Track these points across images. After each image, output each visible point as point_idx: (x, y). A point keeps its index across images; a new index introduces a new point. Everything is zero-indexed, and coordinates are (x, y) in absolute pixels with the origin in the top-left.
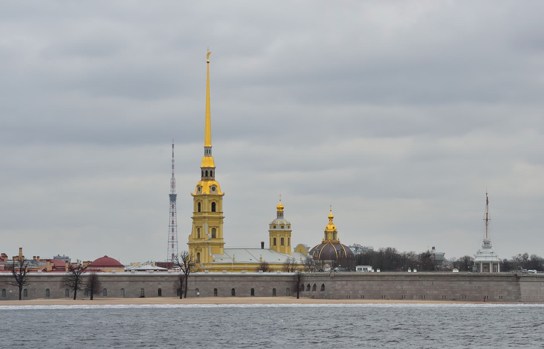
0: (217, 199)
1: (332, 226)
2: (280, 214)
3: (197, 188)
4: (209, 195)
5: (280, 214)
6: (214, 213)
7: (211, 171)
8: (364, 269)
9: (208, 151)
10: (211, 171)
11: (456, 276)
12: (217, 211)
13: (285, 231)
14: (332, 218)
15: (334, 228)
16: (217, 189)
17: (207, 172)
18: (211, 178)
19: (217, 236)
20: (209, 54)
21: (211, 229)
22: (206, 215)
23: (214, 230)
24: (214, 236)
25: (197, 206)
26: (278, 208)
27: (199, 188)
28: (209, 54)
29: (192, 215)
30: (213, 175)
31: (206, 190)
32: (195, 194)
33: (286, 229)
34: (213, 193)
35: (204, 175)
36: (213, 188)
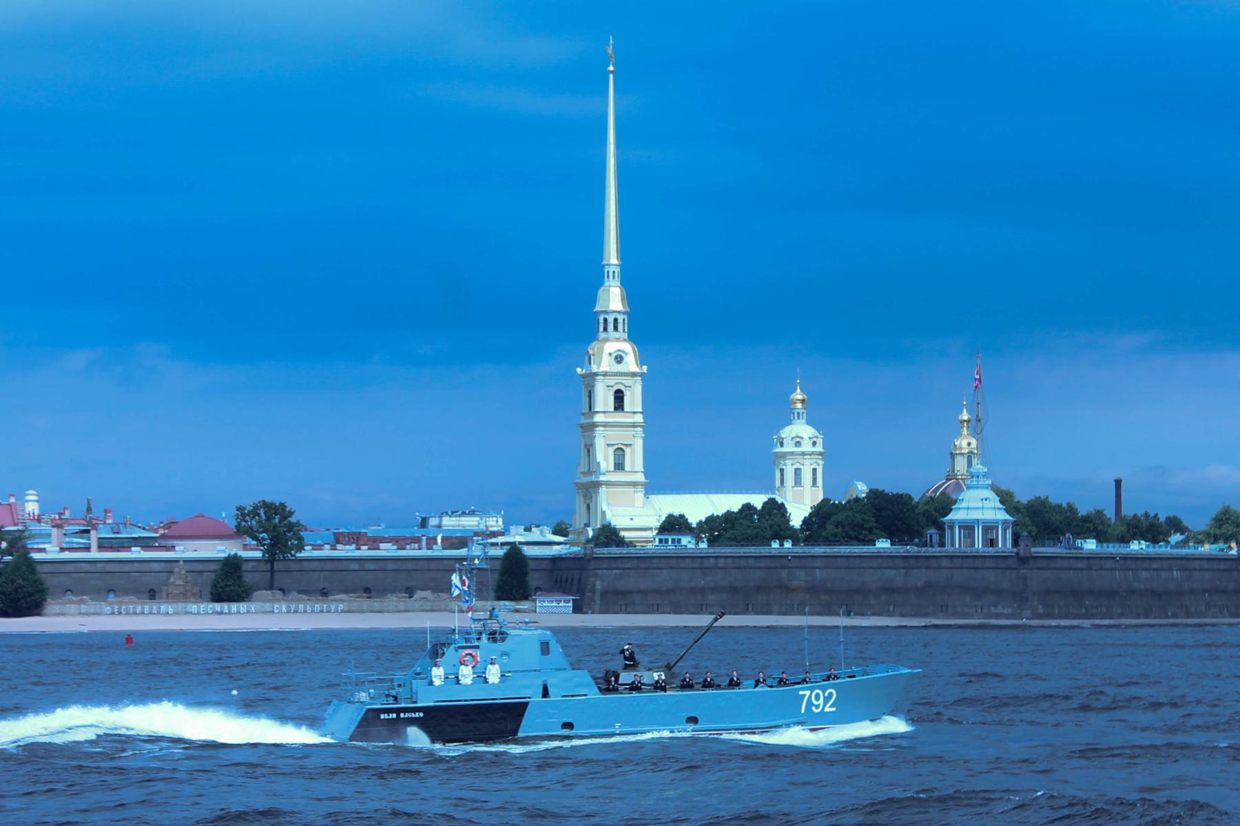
0: (628, 381)
4: (605, 374)
6: (619, 414)
7: (616, 320)
8: (673, 540)
10: (616, 320)
11: (880, 556)
13: (803, 454)
14: (968, 421)
15: (969, 444)
17: (605, 320)
18: (617, 335)
19: (627, 467)
21: (611, 450)
22: (598, 418)
24: (619, 466)
35: (601, 329)
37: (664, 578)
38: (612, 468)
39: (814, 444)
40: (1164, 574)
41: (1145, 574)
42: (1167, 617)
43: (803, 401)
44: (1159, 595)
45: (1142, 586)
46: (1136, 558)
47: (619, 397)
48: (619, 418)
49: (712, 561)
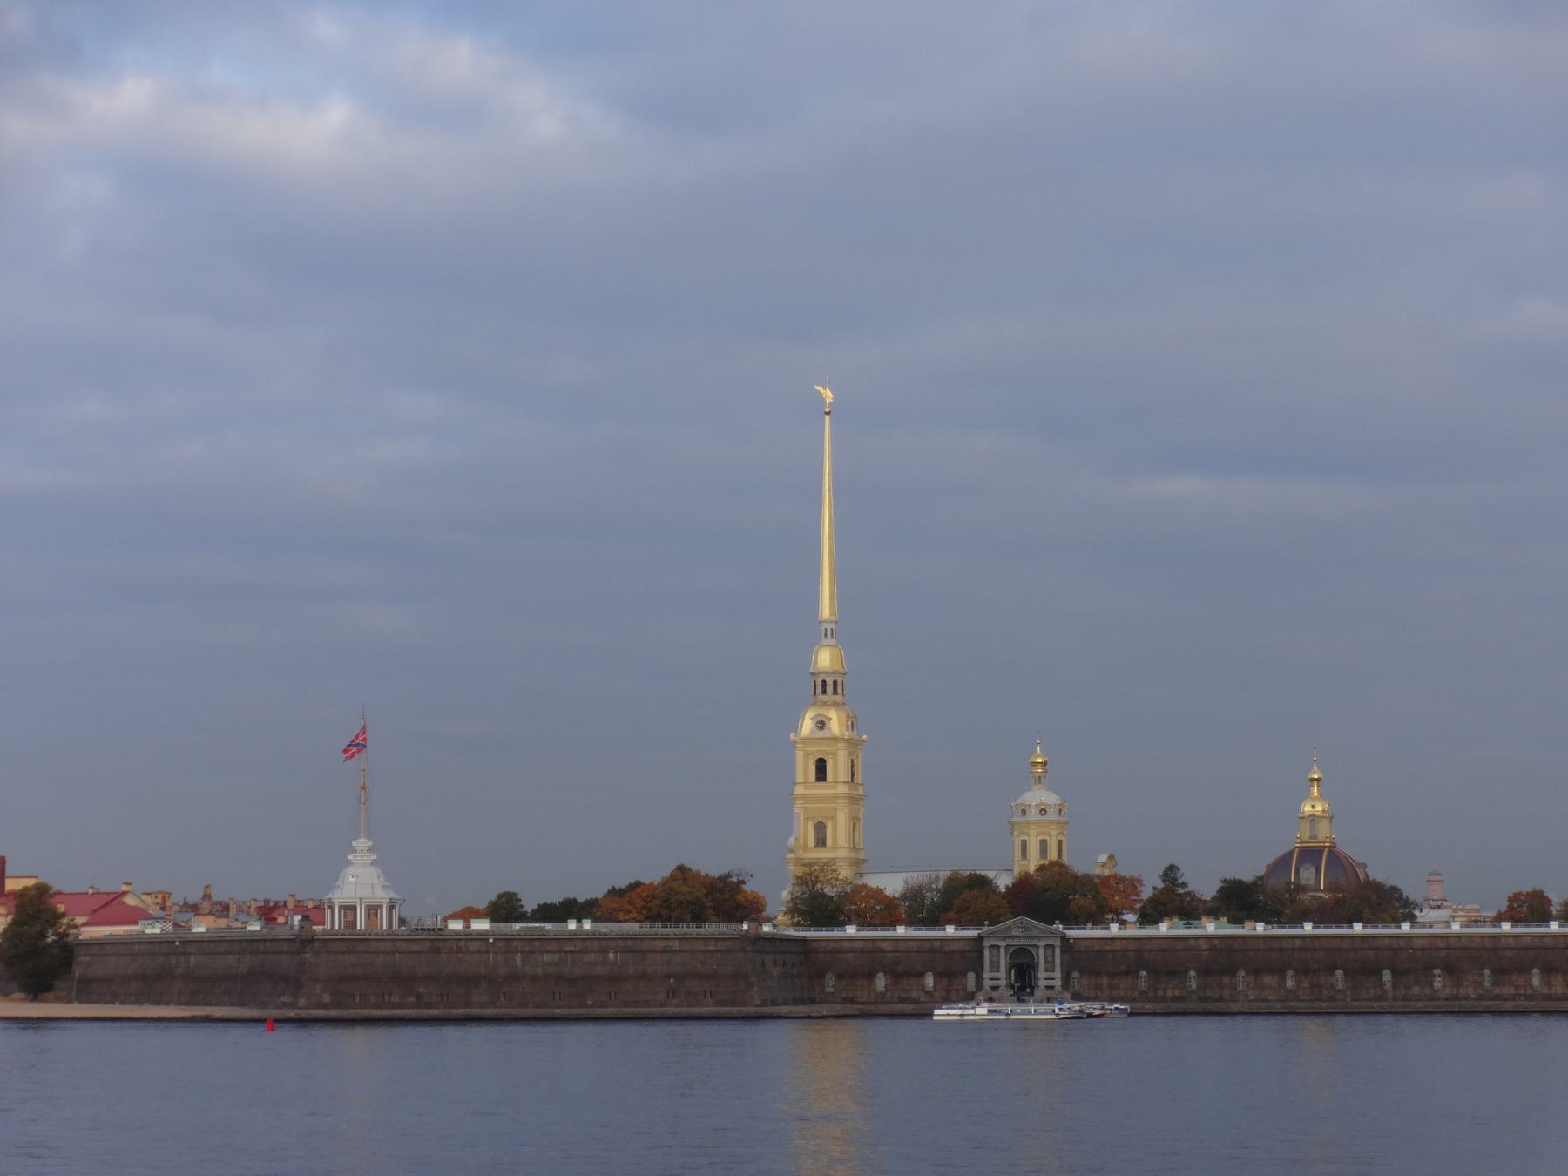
4: (805, 739)
7: (824, 683)
10: (824, 683)
18: (824, 698)
19: (829, 842)
23: (820, 829)
24: (821, 842)
30: (839, 690)
38: (811, 842)
39: (1043, 812)
40: (591, 957)
41: (547, 958)
42: (587, 1006)
43: (1044, 764)
44: (572, 981)
45: (540, 971)
46: (572, 938)
47: (821, 766)
48: (822, 789)
49: (390, 944)
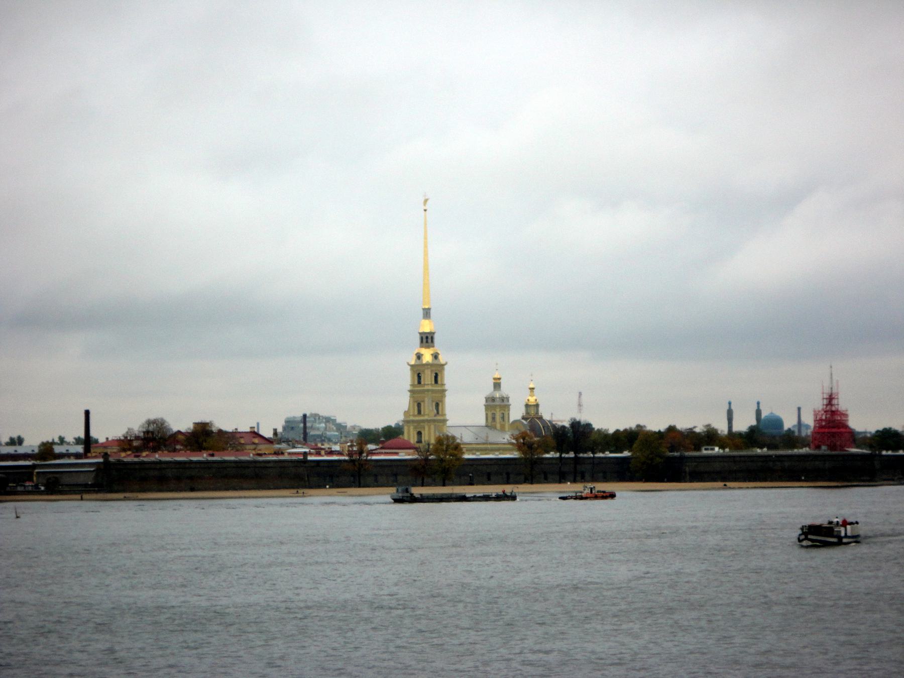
1: (534, 398)
2: (497, 385)
3: (415, 357)
5: (497, 385)
9: (427, 313)
12: (439, 382)
16: (440, 357)
20: (426, 201)
22: (430, 387)
25: (416, 378)
26: (495, 379)
27: (419, 356)
28: (426, 201)
29: (409, 388)
31: (427, 357)
32: (413, 363)
33: (506, 403)
34: (436, 362)
35: (424, 340)
36: (436, 356)
37: (717, 466)
43: (499, 379)
